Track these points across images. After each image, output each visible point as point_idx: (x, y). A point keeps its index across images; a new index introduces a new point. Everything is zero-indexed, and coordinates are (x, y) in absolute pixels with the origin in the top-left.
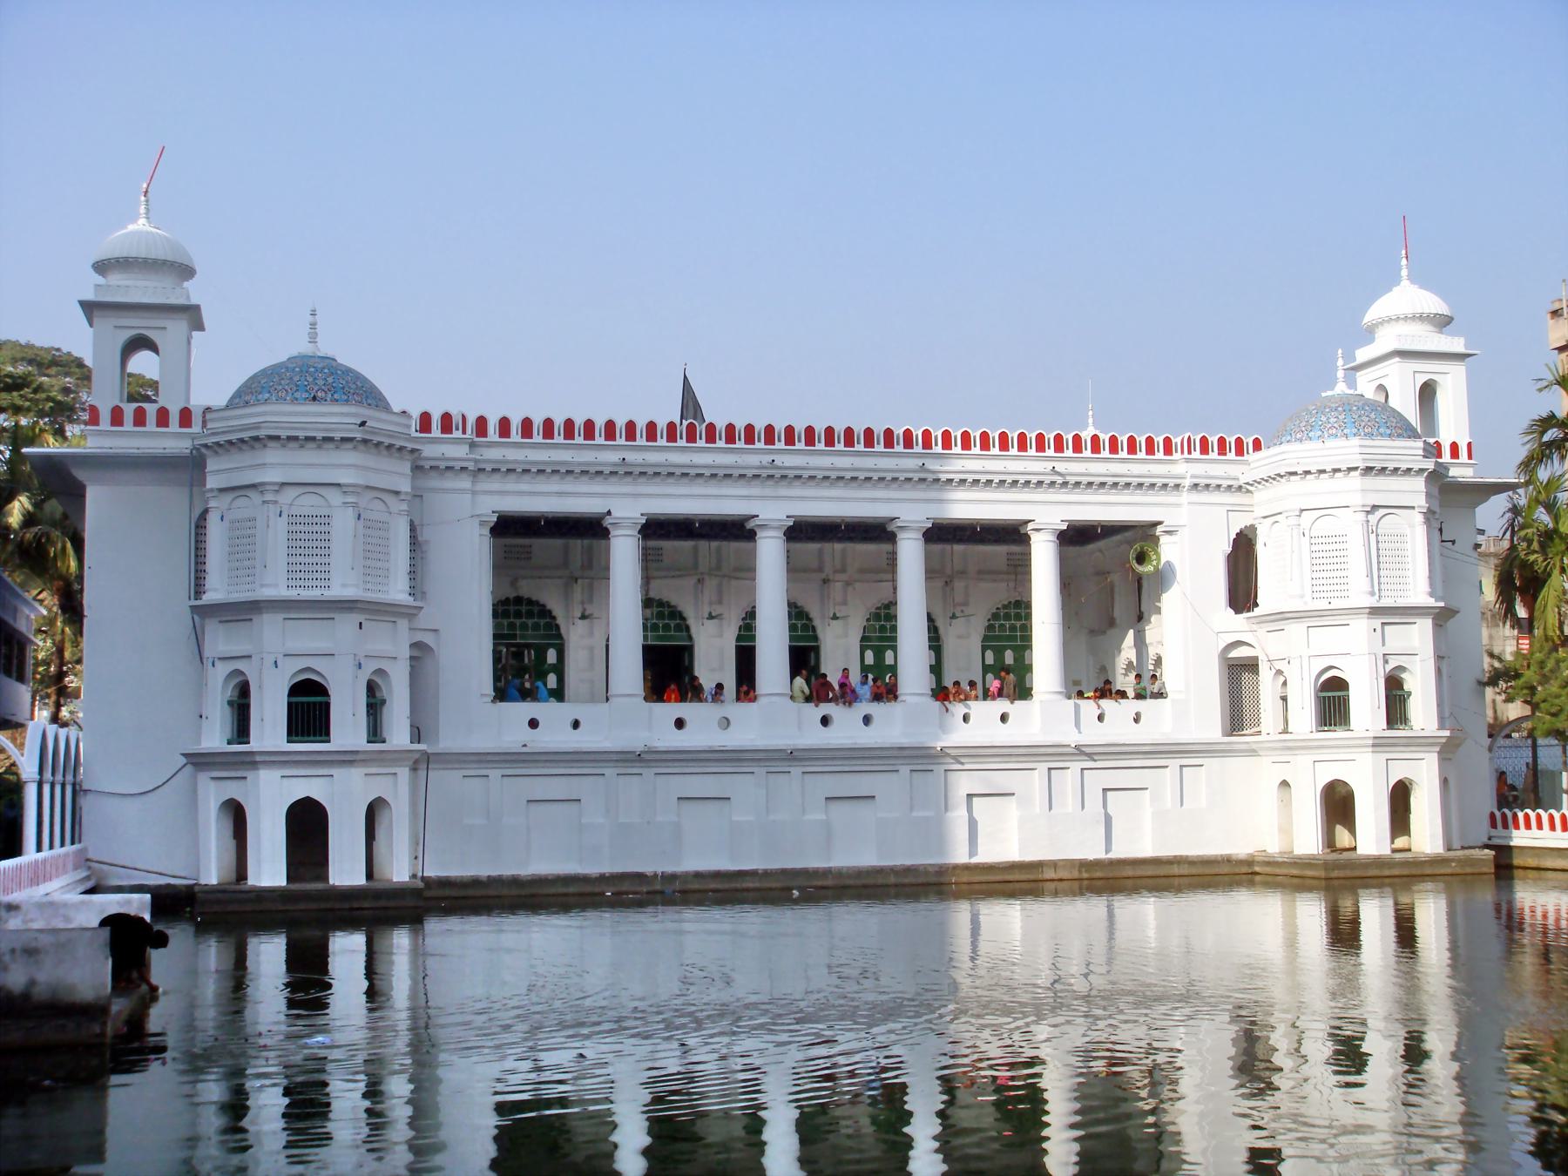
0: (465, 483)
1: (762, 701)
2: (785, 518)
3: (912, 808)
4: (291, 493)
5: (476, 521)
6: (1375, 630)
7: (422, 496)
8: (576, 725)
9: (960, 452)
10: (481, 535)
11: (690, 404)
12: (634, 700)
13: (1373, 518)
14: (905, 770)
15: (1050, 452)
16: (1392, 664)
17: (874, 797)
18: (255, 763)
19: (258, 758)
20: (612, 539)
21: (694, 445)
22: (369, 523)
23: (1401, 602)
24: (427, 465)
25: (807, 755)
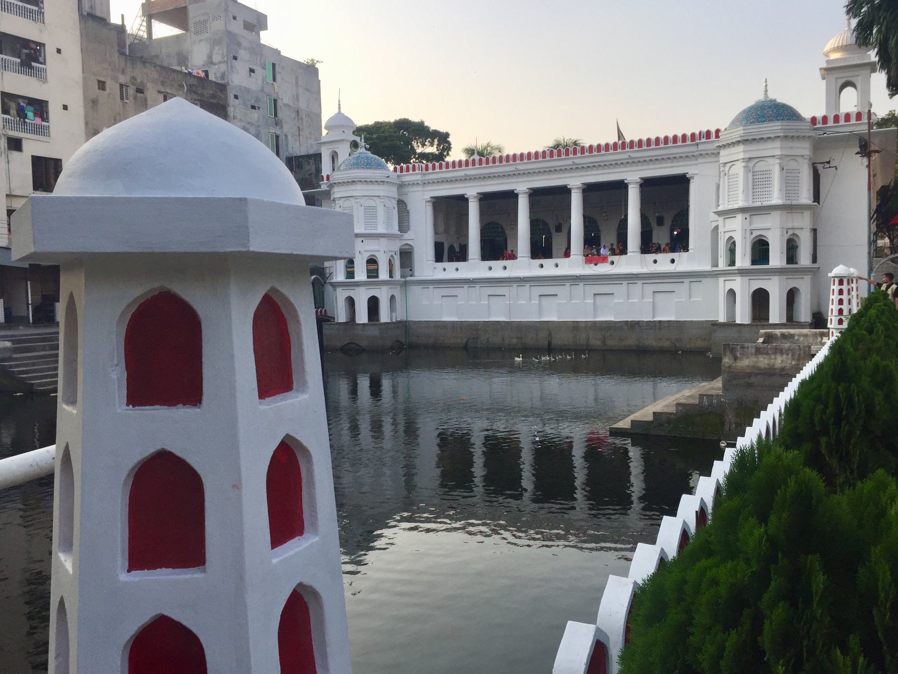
0: (419, 188)
1: (519, 259)
2: (526, 189)
3: (571, 300)
4: (343, 200)
5: (424, 201)
6: (746, 219)
7: (407, 194)
8: (457, 269)
9: (597, 154)
10: (426, 206)
11: (620, 135)
12: (476, 260)
13: (751, 164)
14: (568, 284)
15: (571, 156)
16: (756, 234)
17: (557, 295)
18: (335, 286)
19: (334, 284)
20: (469, 203)
21: (633, 150)
22: (789, 171)
23: (765, 204)
24: (406, 183)
25: (527, 279)
